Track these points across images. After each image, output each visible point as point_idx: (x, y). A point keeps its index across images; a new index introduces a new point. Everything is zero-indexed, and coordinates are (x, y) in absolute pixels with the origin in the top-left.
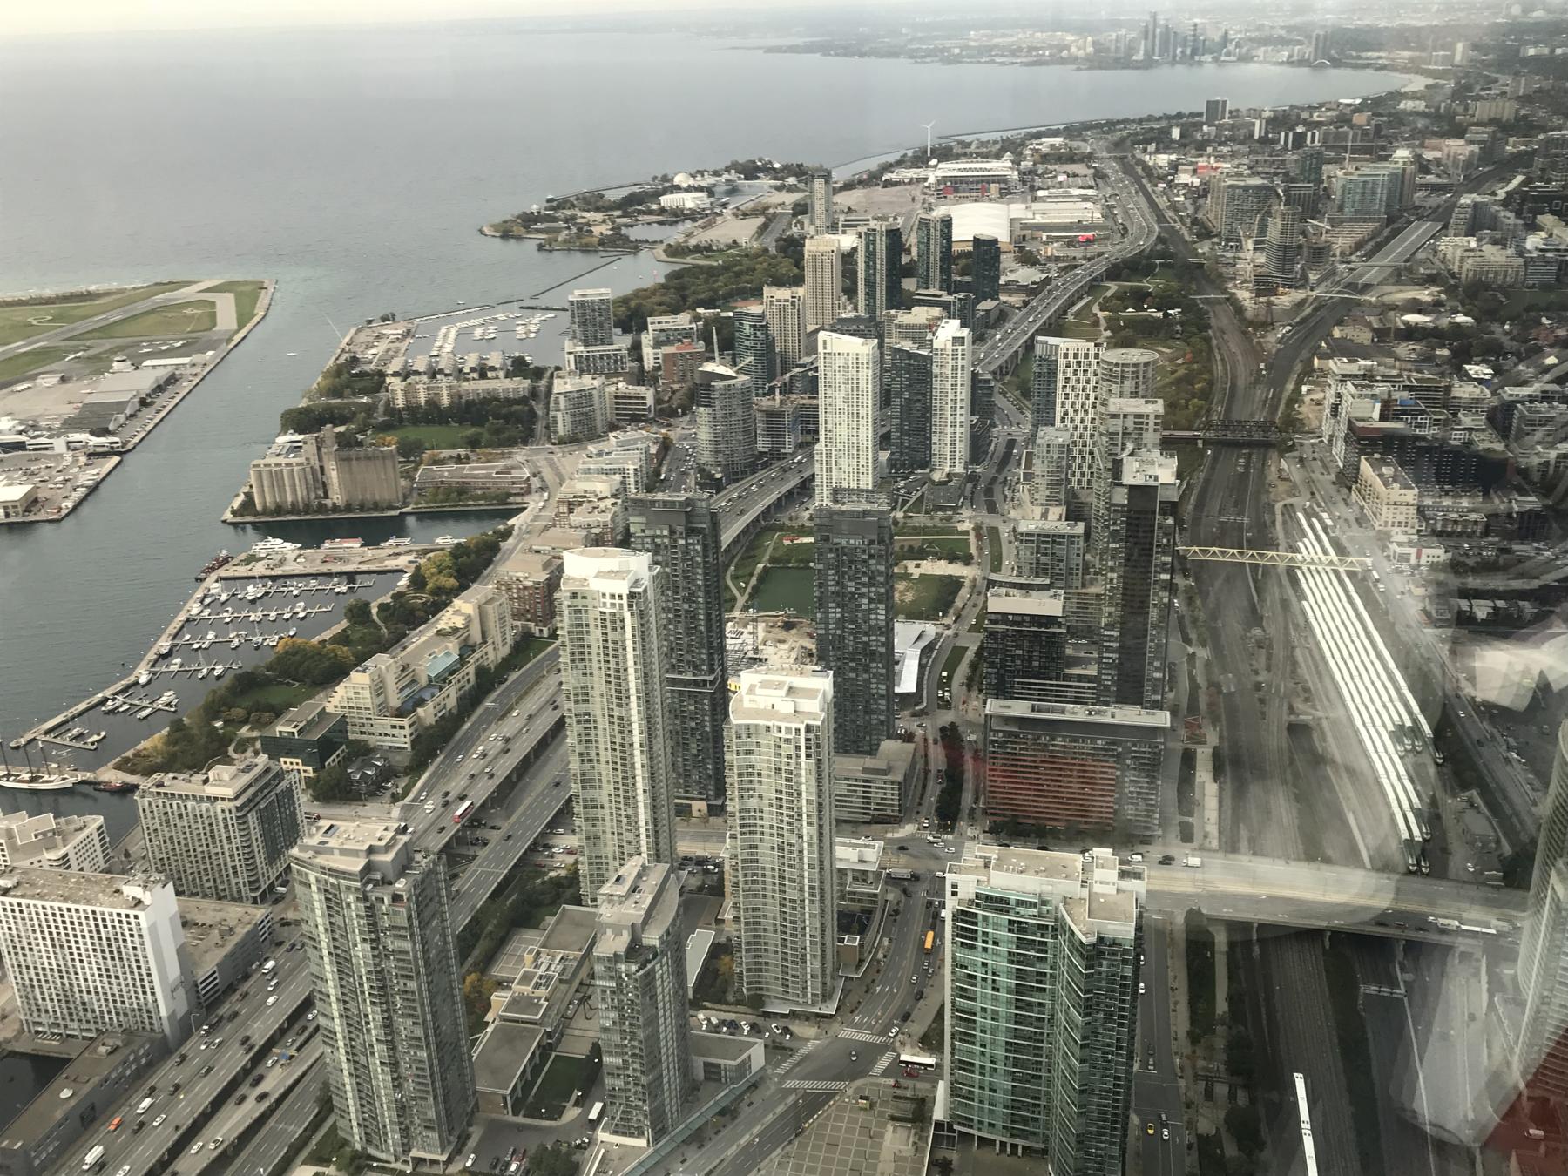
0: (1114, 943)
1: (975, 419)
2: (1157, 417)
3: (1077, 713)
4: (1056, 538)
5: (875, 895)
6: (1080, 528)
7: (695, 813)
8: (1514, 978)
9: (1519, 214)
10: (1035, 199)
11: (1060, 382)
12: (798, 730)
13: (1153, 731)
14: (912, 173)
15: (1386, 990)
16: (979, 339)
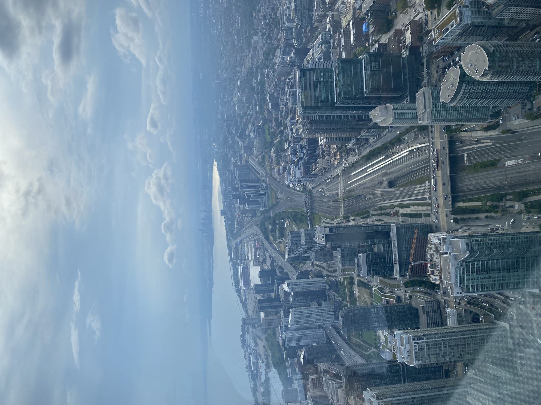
0: (467, 244)
1: (310, 277)
2: (305, 230)
3: (395, 250)
4: (343, 256)
5: (465, 310)
6: (338, 249)
7: (447, 368)
8: (455, 126)
9: (246, 139)
10: (248, 259)
11: (299, 255)
12: (415, 343)
13: (397, 228)
14: (243, 293)
15: (466, 159)
16: (288, 279)
